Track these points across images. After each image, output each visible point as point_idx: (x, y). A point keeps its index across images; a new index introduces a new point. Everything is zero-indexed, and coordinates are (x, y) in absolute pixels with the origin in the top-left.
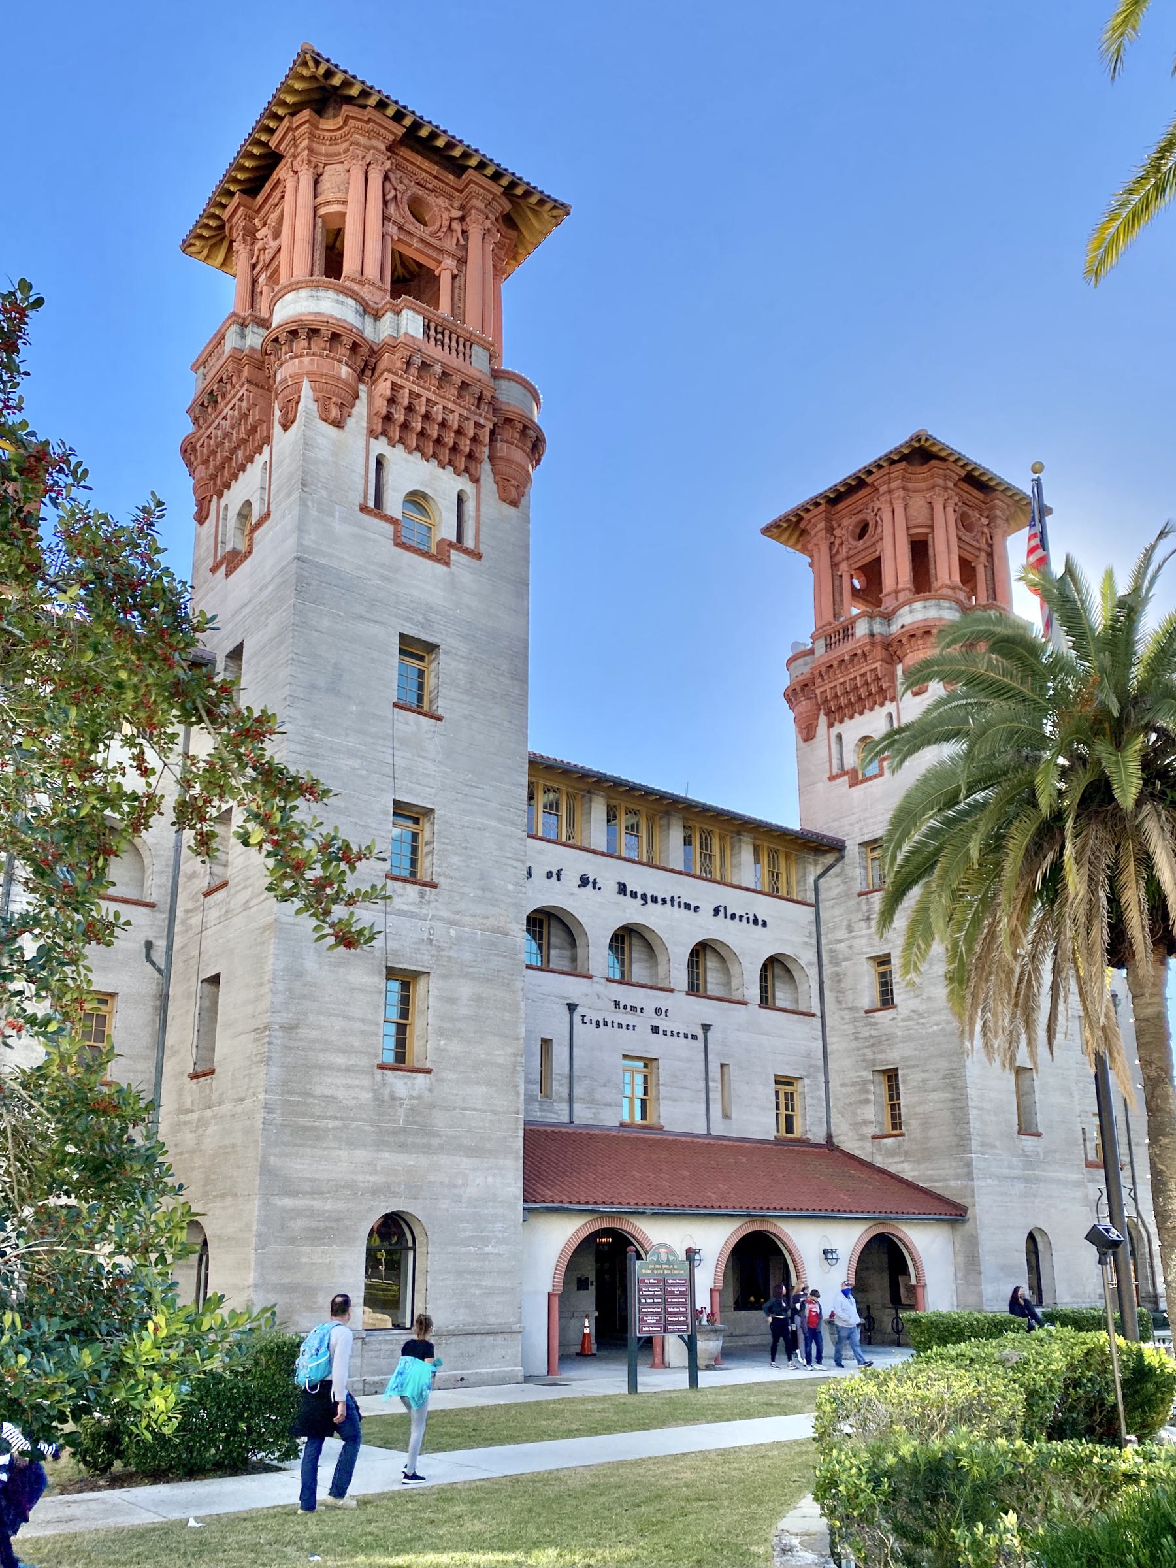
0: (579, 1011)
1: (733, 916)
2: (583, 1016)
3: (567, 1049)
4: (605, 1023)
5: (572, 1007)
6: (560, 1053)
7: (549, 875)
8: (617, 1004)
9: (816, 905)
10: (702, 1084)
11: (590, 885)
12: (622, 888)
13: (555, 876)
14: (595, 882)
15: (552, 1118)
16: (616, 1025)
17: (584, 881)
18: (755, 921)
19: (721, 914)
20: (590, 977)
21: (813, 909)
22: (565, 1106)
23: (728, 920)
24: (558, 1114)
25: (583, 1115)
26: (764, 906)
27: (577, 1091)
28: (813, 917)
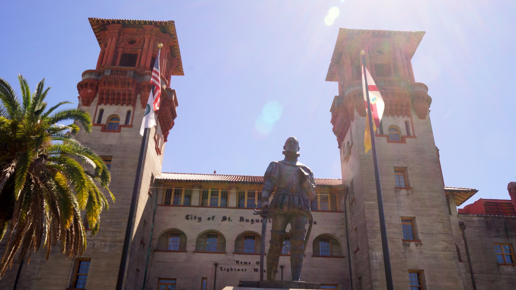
0: (220, 266)
2: (221, 268)
4: (232, 269)
7: (209, 219)
8: (237, 262)
9: (345, 212)
11: (227, 221)
12: (242, 219)
13: (211, 219)
14: (229, 219)
16: (237, 270)
20: (225, 253)
21: (344, 214)
28: (344, 217)
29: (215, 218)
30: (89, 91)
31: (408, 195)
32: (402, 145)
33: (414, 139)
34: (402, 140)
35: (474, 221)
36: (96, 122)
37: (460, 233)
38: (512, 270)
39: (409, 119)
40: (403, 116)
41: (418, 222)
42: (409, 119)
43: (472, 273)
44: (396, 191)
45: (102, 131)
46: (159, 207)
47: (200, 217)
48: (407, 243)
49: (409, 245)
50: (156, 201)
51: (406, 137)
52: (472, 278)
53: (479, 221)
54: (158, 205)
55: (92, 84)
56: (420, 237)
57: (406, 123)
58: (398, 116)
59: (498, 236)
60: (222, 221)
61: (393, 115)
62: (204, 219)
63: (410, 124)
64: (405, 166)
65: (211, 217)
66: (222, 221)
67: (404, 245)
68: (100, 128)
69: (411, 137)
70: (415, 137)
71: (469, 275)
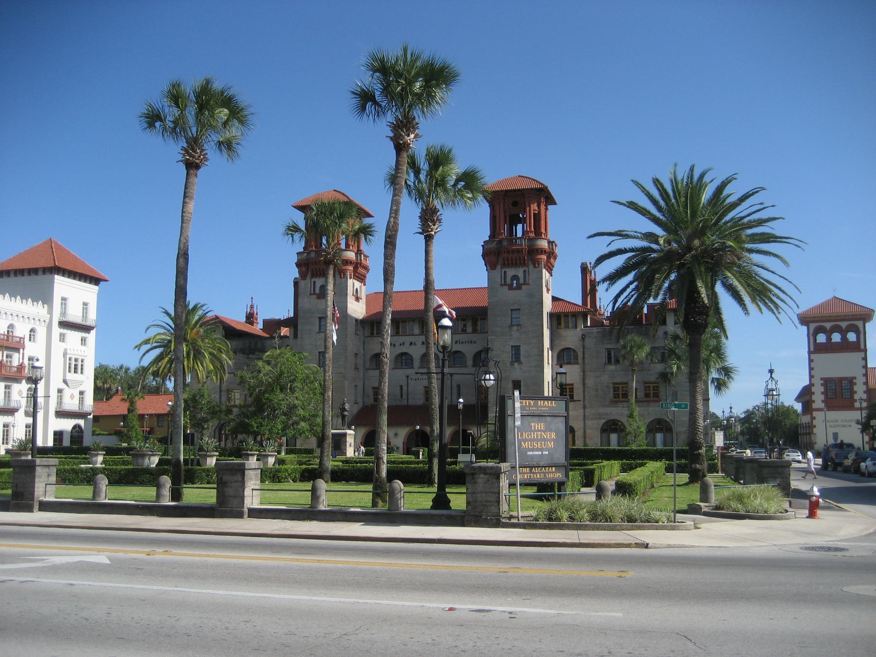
1: (462, 343)
3: (406, 387)
4: (418, 379)
5: (408, 377)
6: (405, 388)
10: (450, 391)
15: (402, 404)
17: (411, 344)
18: (471, 342)
19: (461, 342)
20: (414, 368)
22: (406, 400)
23: (461, 344)
24: (405, 403)
25: (411, 402)
26: (474, 337)
27: (409, 397)
29: (405, 344)
30: (304, 269)
31: (518, 330)
32: (518, 292)
33: (527, 286)
34: (519, 287)
35: (593, 333)
36: (312, 292)
37: (581, 343)
38: (615, 367)
39: (527, 269)
40: (523, 267)
41: (522, 348)
42: (527, 269)
43: (584, 372)
44: (510, 328)
45: (317, 298)
46: (366, 338)
47: (395, 343)
48: (512, 363)
49: (513, 365)
50: (364, 334)
51: (522, 284)
52: (584, 375)
53: (597, 332)
54: (366, 337)
55: (305, 264)
56: (522, 359)
57: (525, 271)
58: (519, 267)
59: (610, 343)
60: (410, 345)
61: (515, 267)
62: (397, 345)
63: (527, 273)
64: (518, 308)
65: (402, 343)
66: (410, 345)
67: (511, 364)
68: (315, 296)
69: (527, 284)
70: (528, 284)
71: (582, 373)
